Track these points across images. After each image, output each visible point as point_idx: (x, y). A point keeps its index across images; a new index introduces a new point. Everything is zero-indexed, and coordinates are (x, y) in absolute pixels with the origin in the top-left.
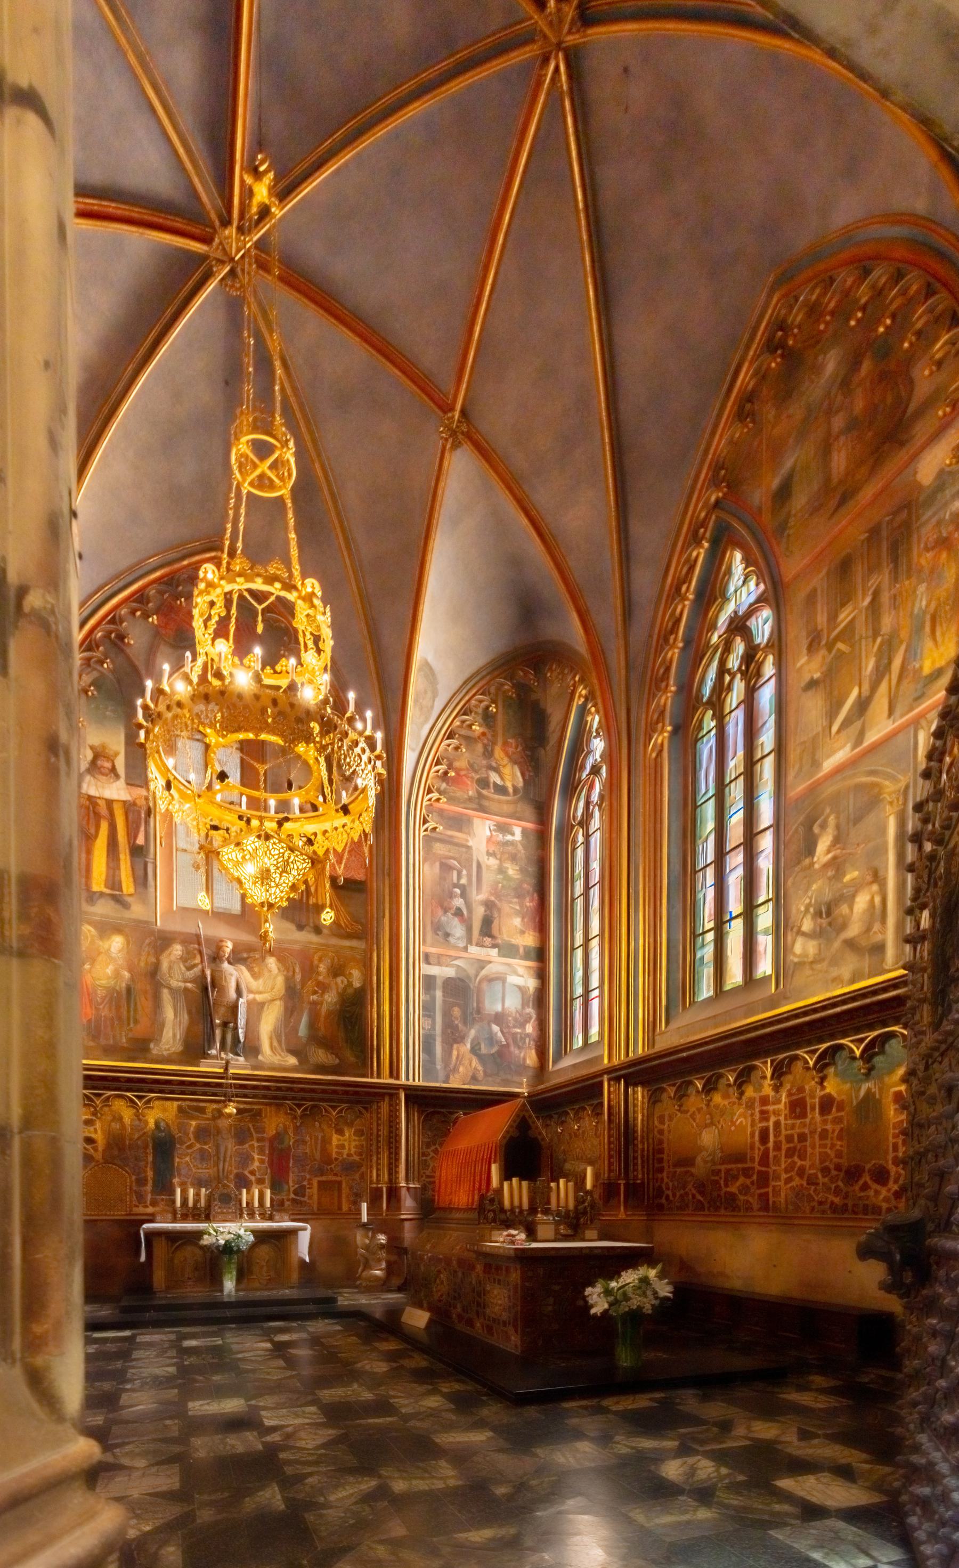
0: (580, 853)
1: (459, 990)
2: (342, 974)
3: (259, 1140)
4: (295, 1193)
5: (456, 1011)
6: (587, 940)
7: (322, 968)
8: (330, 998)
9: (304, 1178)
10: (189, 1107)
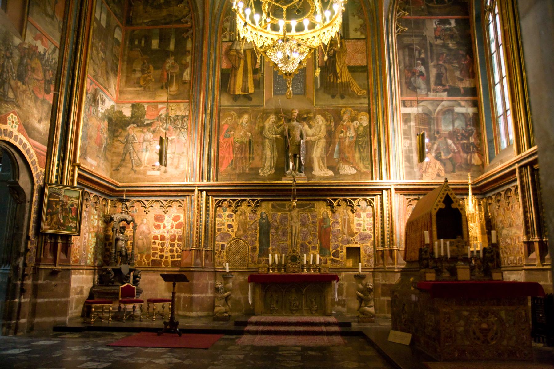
0: (491, 27)
2: (356, 119)
8: (351, 133)
10: (278, 205)
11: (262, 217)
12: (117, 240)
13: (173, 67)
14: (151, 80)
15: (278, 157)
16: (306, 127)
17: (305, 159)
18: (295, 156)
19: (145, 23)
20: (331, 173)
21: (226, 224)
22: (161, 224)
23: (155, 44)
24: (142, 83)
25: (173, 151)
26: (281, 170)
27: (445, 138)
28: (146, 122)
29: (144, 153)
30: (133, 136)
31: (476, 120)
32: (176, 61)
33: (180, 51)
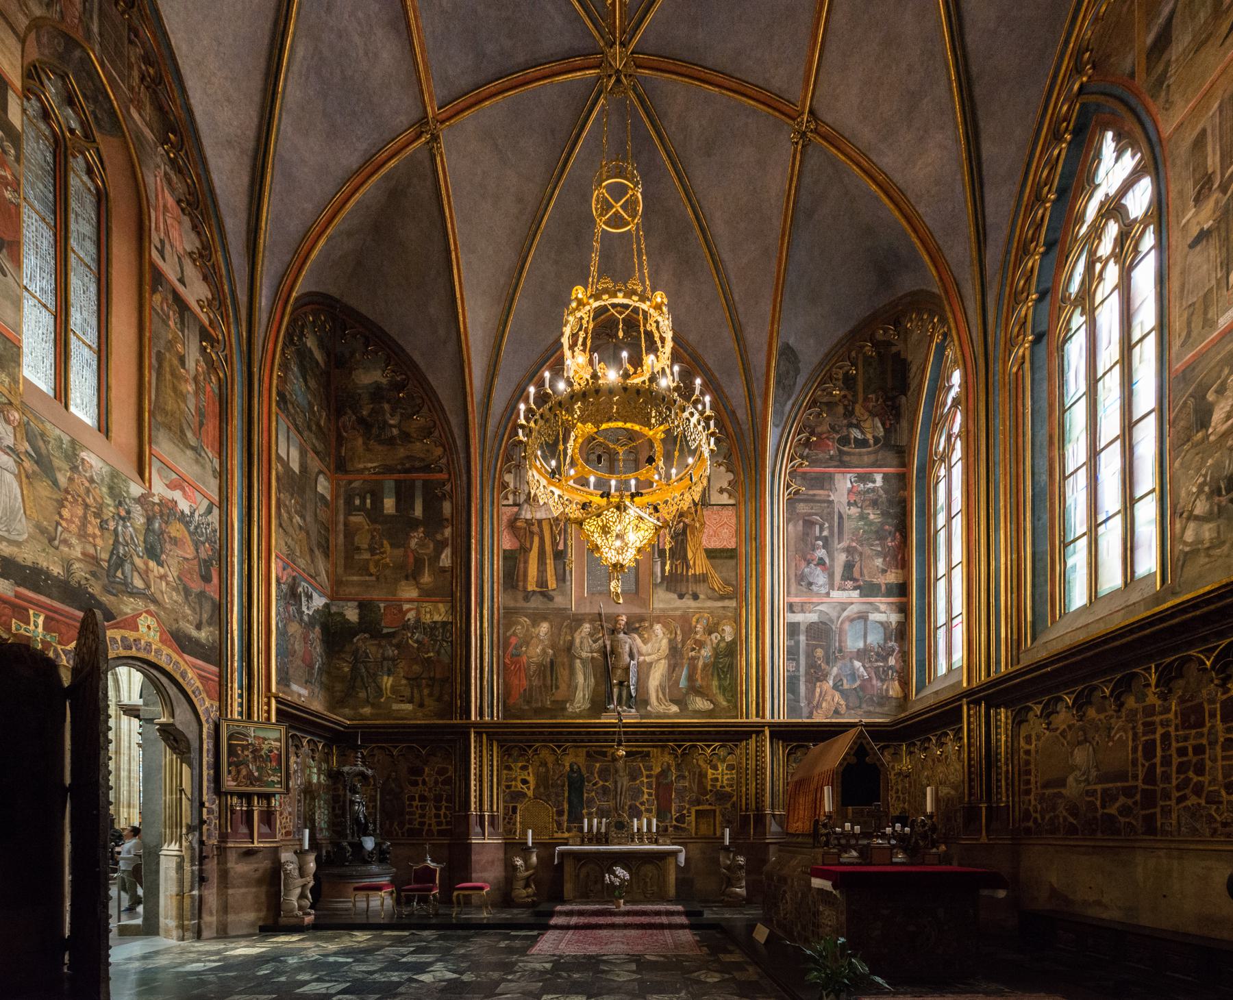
1: (820, 632)
3: (648, 777)
4: (677, 820)
5: (819, 653)
6: (950, 569)
7: (699, 628)
8: (706, 652)
9: (684, 808)
11: (572, 769)
12: (352, 803)
13: (421, 544)
14: (386, 566)
15: (597, 684)
16: (639, 641)
17: (637, 690)
18: (621, 684)
19: (369, 469)
20: (674, 709)
21: (519, 779)
22: (420, 779)
23: (389, 504)
24: (373, 570)
25: (432, 674)
26: (599, 704)
27: (851, 659)
28: (385, 631)
29: (385, 678)
30: (365, 652)
31: (901, 633)
32: (427, 534)
33: (433, 520)
